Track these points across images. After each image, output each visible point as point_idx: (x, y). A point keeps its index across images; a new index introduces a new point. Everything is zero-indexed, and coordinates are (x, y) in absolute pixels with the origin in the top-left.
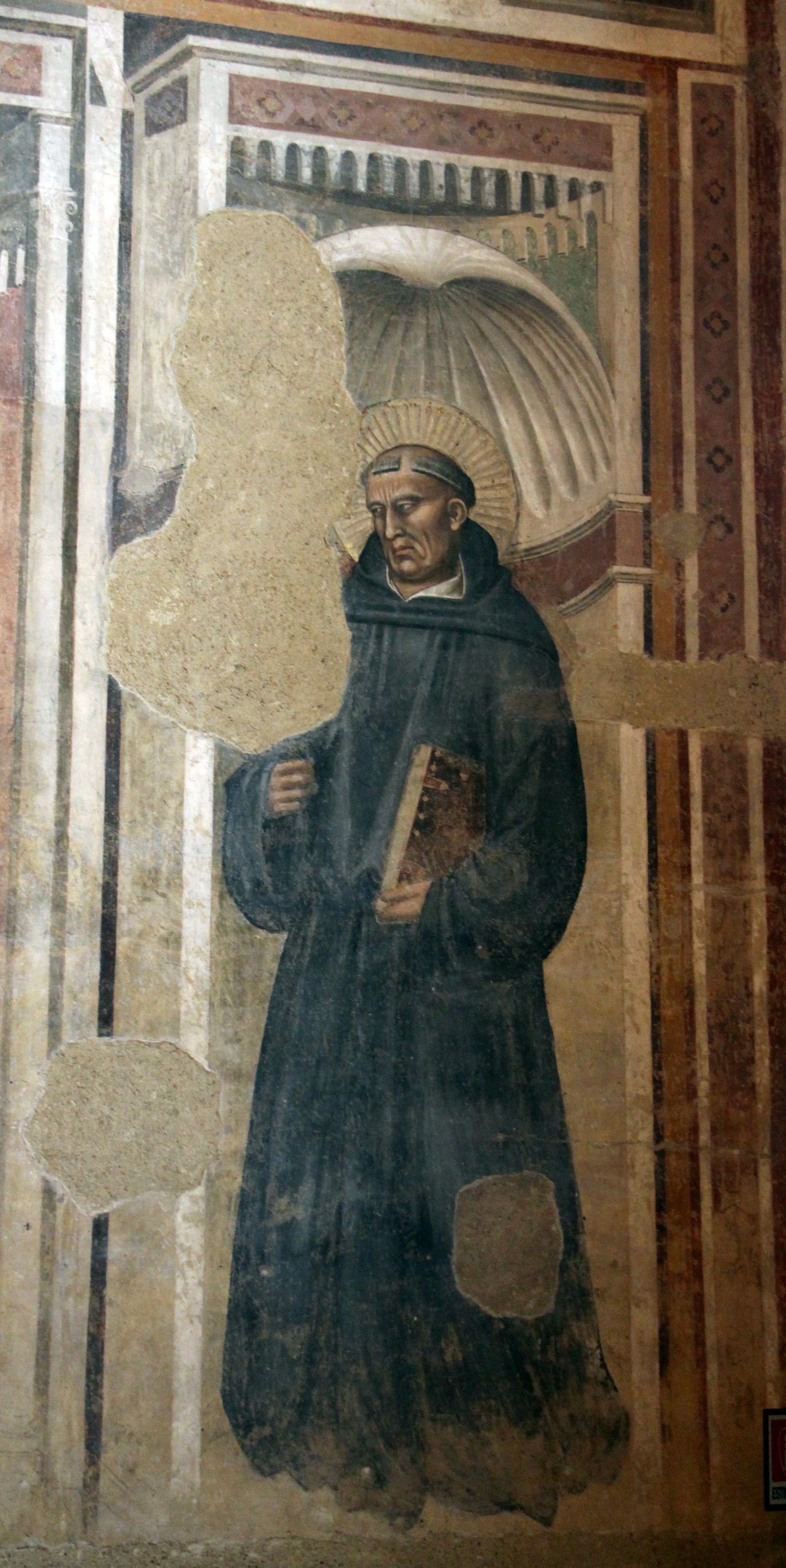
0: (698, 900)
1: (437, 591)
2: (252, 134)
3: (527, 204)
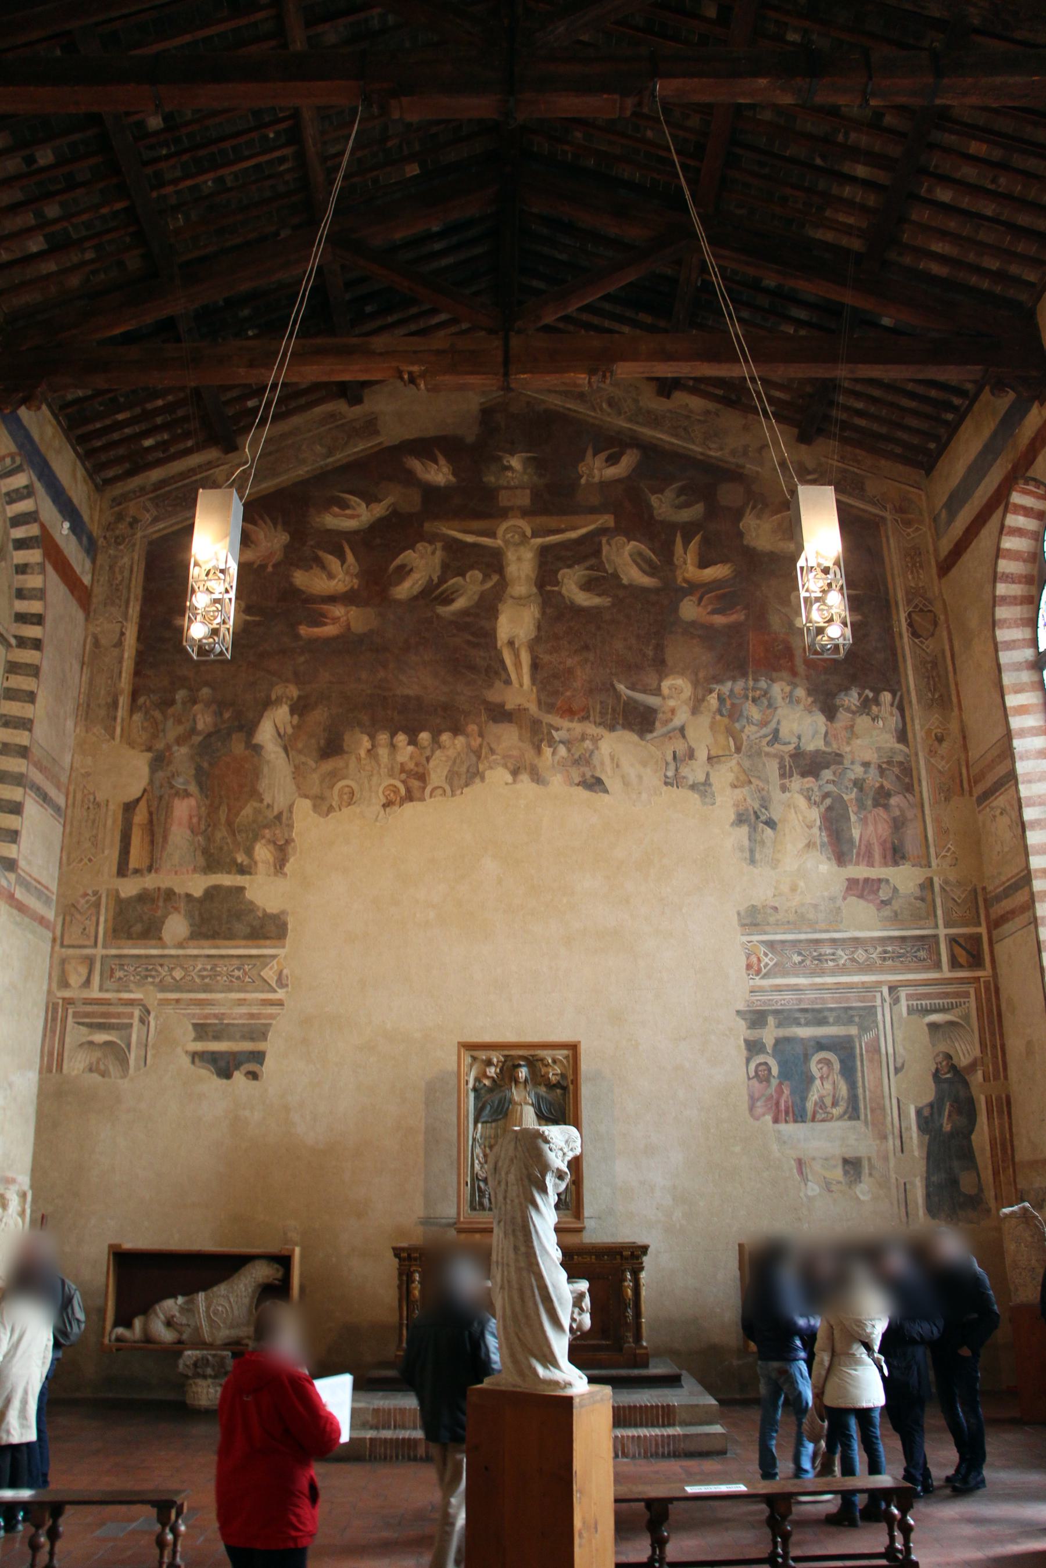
0: (996, 1123)
1: (948, 1076)
2: (910, 1003)
3: (957, 1007)
